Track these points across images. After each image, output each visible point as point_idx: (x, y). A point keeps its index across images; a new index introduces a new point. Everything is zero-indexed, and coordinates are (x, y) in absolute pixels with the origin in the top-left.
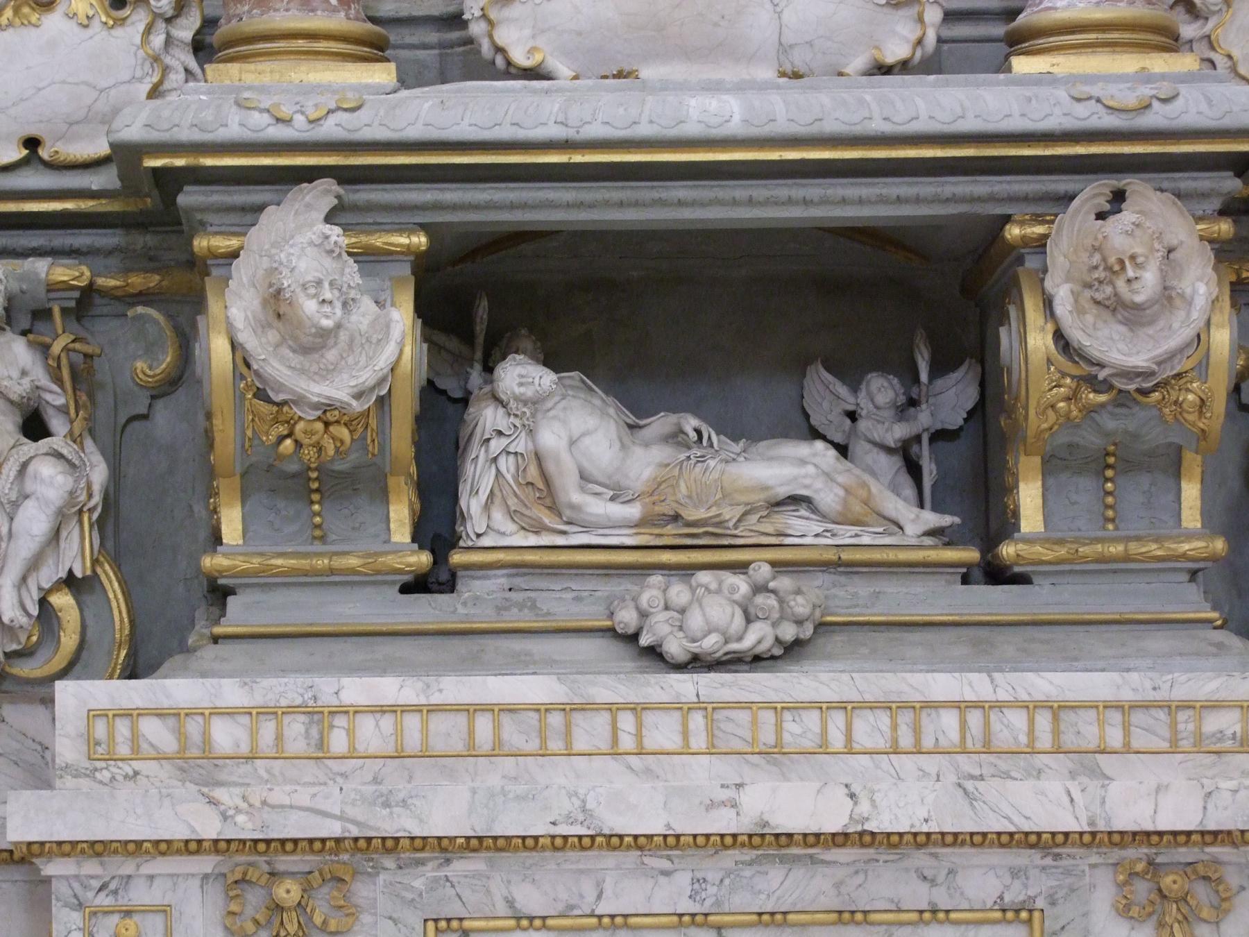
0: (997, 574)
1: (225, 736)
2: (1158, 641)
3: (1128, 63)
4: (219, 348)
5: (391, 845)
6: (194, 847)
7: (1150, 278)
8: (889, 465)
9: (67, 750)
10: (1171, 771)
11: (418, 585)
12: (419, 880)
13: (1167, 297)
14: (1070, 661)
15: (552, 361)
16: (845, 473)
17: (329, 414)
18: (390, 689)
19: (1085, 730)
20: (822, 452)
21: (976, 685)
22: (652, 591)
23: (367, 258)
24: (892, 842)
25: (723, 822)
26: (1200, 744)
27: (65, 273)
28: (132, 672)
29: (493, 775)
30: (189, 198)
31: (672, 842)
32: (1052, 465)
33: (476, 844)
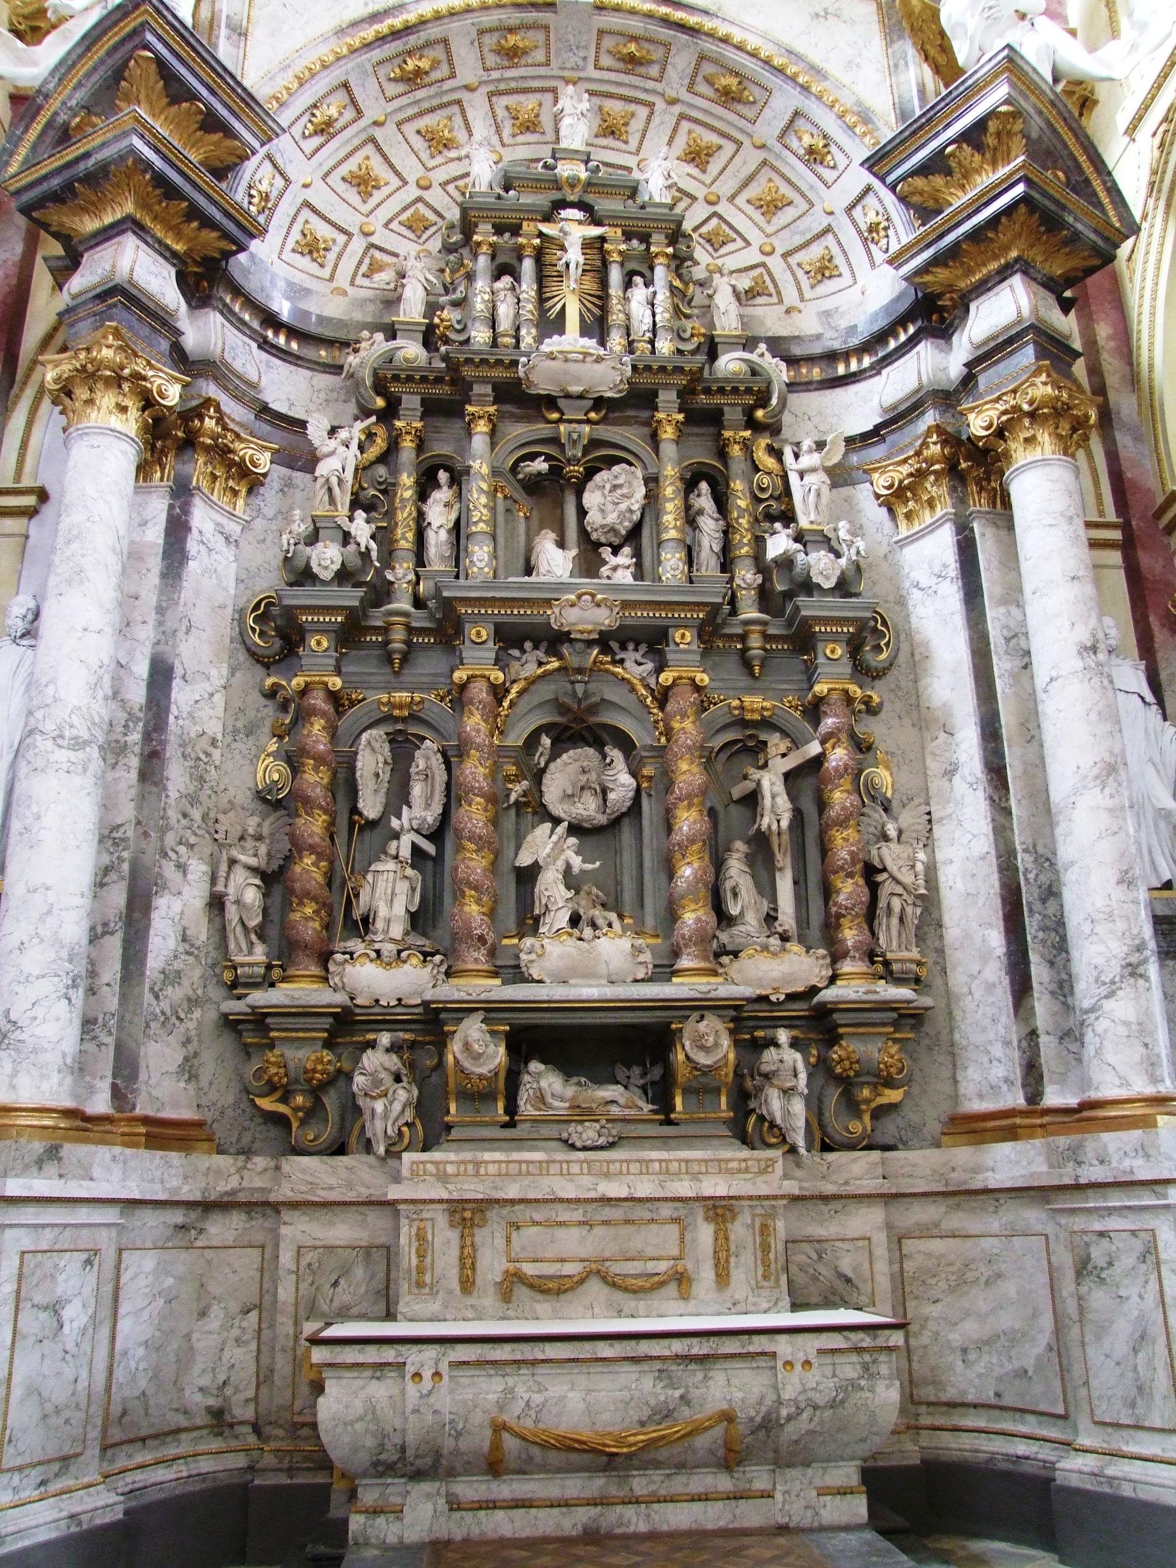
0: (669, 1122)
1: (450, 1169)
2: (715, 1142)
3: (705, 980)
4: (450, 1058)
5: (497, 1201)
6: (441, 1201)
7: (711, 1039)
8: (638, 1091)
9: (405, 1172)
10: (719, 1179)
11: (505, 1126)
12: (505, 1211)
13: (716, 1045)
14: (690, 1148)
15: (544, 1061)
16: (627, 1094)
17: (481, 1077)
18: (498, 1156)
19: (695, 1167)
20: (620, 1088)
21: (664, 1155)
22: (572, 1128)
23: (492, 1033)
24: (640, 1200)
25: (593, 1195)
27: (408, 1036)
28: (424, 1150)
29: (526, 1181)
30: (443, 1016)
31: (578, 1201)
32: (686, 1092)
33: (522, 1201)
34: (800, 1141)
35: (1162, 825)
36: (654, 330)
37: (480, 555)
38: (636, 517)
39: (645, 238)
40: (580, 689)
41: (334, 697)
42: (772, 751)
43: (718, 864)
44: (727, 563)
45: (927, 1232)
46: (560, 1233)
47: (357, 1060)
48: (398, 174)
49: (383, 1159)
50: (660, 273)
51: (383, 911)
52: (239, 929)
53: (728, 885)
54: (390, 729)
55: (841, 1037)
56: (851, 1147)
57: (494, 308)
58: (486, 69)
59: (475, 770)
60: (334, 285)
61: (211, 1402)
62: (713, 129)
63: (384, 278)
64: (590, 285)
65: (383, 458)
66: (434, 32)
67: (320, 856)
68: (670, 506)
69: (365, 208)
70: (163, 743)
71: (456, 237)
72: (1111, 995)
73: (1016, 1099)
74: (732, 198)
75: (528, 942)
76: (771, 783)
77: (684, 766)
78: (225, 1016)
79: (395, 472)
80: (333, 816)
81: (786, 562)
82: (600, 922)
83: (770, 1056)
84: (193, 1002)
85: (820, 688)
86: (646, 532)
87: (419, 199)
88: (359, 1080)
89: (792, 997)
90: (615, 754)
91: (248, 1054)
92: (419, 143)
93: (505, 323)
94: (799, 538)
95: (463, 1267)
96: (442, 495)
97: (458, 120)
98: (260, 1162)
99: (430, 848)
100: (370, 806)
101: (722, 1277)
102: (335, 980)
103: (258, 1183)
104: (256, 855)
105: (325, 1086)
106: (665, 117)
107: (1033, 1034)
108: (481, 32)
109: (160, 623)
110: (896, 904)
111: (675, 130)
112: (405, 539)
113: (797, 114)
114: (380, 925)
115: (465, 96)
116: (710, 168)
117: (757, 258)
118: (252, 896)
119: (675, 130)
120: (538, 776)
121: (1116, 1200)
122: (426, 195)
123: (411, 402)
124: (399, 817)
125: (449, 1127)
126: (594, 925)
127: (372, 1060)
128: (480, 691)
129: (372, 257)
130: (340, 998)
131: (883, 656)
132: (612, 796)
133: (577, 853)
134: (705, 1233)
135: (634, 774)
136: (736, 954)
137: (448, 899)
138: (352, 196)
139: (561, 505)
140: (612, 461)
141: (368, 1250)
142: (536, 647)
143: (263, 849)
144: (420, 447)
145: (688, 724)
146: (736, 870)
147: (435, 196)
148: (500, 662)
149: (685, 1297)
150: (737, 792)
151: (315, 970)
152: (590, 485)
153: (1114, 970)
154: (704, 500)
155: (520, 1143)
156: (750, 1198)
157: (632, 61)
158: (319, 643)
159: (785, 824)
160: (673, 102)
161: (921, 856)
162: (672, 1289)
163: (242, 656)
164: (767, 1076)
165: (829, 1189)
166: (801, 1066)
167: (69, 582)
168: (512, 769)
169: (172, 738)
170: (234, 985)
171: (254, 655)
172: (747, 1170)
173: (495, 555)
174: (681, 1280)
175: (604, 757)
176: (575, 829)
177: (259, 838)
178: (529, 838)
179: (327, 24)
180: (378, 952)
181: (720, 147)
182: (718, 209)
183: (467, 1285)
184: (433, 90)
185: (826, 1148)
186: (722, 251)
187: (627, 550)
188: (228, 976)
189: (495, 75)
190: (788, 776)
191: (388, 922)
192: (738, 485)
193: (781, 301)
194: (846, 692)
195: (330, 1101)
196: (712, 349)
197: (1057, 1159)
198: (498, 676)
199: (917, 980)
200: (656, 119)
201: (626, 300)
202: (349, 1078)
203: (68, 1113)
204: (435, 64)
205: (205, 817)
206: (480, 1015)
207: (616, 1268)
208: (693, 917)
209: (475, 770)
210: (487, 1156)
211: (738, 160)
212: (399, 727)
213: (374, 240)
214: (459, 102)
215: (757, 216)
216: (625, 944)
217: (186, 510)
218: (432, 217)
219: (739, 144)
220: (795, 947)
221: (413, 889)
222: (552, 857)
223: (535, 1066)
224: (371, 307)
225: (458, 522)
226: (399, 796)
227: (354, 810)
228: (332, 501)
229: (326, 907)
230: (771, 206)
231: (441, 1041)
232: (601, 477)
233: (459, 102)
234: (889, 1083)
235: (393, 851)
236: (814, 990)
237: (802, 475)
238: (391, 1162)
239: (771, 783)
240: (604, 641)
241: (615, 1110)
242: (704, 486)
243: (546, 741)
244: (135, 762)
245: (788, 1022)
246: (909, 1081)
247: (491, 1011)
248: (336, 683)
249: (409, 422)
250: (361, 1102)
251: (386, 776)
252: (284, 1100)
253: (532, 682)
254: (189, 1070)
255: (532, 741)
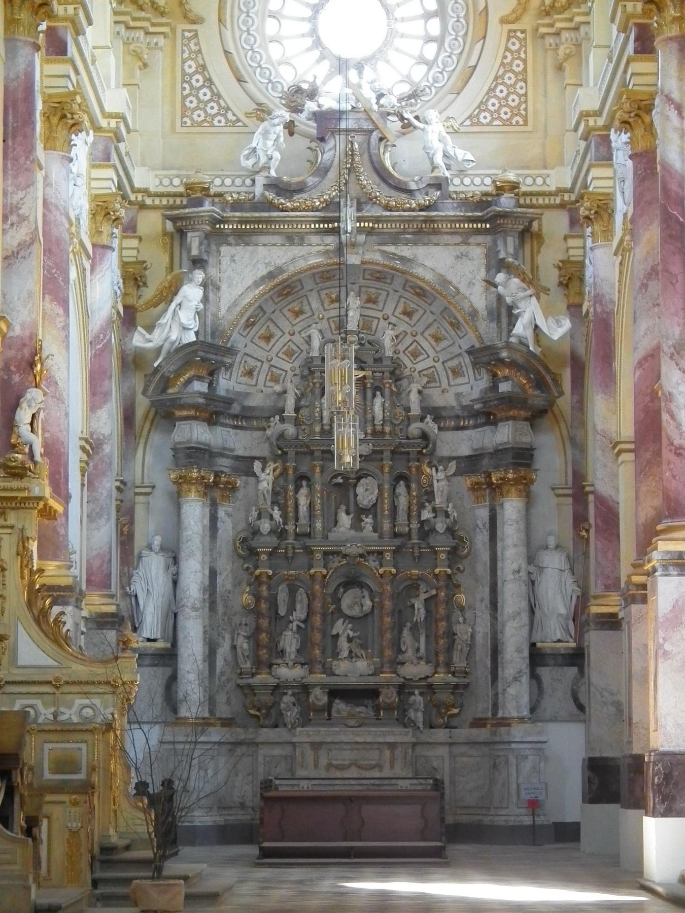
0: (380, 719)
1: (311, 733)
7: (390, 695)
8: (371, 708)
9: (297, 733)
11: (328, 720)
13: (392, 696)
14: (384, 727)
18: (325, 729)
20: (364, 708)
23: (323, 692)
26: (396, 735)
27: (297, 691)
31: (348, 743)
32: (385, 709)
34: (421, 726)
35: (560, 618)
36: (384, 420)
37: (318, 525)
38: (375, 502)
39: (383, 373)
40: (353, 571)
41: (270, 577)
42: (421, 591)
43: (400, 632)
44: (409, 517)
45: (463, 755)
46: (344, 752)
47: (281, 699)
48: (281, 330)
49: (290, 730)
50: (387, 391)
51: (288, 650)
52: (241, 656)
53: (402, 640)
54: (287, 583)
55: (435, 693)
56: (440, 727)
57: (322, 413)
58: (317, 284)
59: (317, 605)
60: (258, 387)
61: (241, 800)
62: (414, 303)
63: (278, 388)
64: (360, 400)
65: (281, 474)
66: (294, 279)
67: (267, 633)
68: (386, 501)
69: (268, 348)
70: (216, 598)
71: (306, 372)
72: (509, 686)
73: (490, 715)
74: (422, 334)
75: (335, 663)
76: (419, 604)
77: (387, 602)
78: (238, 685)
79: (286, 480)
80: (270, 618)
81: (428, 521)
82: (359, 654)
83: (413, 698)
84: (228, 680)
85: (437, 571)
86: (379, 505)
87: (290, 340)
88: (283, 705)
89: (421, 679)
90: (366, 593)
91: (246, 697)
92: (288, 314)
93: (325, 421)
94: (434, 510)
95: (315, 762)
96: (304, 491)
97: (305, 302)
98: (251, 730)
99: (303, 625)
100: (282, 611)
101: (392, 767)
102: (273, 673)
103: (251, 737)
104: (246, 632)
105: (271, 707)
106: (393, 297)
107: (497, 694)
108: (314, 275)
109: (211, 555)
110: (459, 647)
111: (398, 301)
112: (291, 509)
113: (445, 308)
114: (287, 654)
115: (308, 294)
116: (413, 318)
117: (433, 363)
118: (245, 646)
119: (398, 301)
120: (340, 600)
121: (502, 747)
122: (294, 338)
123: (291, 454)
124: (292, 616)
125: (310, 720)
126: (357, 656)
127: (288, 699)
128: (319, 576)
129: (272, 371)
130: (276, 681)
131: (466, 551)
132: (364, 608)
133: (351, 630)
134: (387, 753)
135: (372, 601)
136: (403, 664)
137: (309, 645)
138: (263, 344)
139: (348, 490)
140: (366, 476)
141: (286, 757)
142: (338, 556)
143: (248, 629)
144: (295, 469)
145: (388, 588)
146: (406, 633)
147: (296, 338)
148: (325, 567)
149: (381, 771)
150: (409, 604)
151: (267, 670)
152: (359, 484)
153: (511, 679)
154: (401, 489)
155: (332, 725)
156: (401, 743)
157: (378, 279)
158: (264, 557)
159: (422, 619)
160: (397, 291)
161: (470, 630)
162: (377, 769)
163: (236, 557)
164: (411, 705)
165: (431, 740)
166: (422, 701)
167: (189, 556)
168: (329, 600)
169: (218, 596)
170: (241, 674)
171: (239, 556)
172: (401, 734)
173: (323, 522)
174: (379, 766)
175: (363, 592)
176: (352, 619)
177: (246, 625)
178: (336, 624)
179: (250, 282)
180: (287, 664)
181: (417, 310)
182: (417, 338)
183: (316, 766)
184: (295, 295)
185: (431, 727)
186: (418, 360)
187: (371, 516)
188: (238, 671)
189: (321, 285)
190: (426, 600)
191: (290, 653)
192: (413, 486)
193: (440, 387)
194: (446, 571)
195: (273, 711)
196: (409, 420)
197: (494, 734)
198: (324, 572)
199: (466, 673)
200: (390, 297)
201: (373, 405)
202: (279, 704)
203: (204, 719)
204: (296, 286)
205: (229, 619)
206: (319, 687)
207: (360, 763)
208: (388, 653)
209: (317, 605)
210: (322, 729)
211: (425, 317)
212: (291, 582)
213: (272, 363)
214: (306, 296)
215: (433, 343)
216: (365, 663)
217: (216, 512)
218: (295, 348)
219: (425, 311)
220: (423, 663)
221: (297, 641)
222: (344, 632)
223: (337, 701)
224: (273, 397)
225: (310, 503)
226: (292, 608)
227: (277, 613)
228: (265, 499)
229: (270, 649)
230: (438, 339)
231: (308, 694)
232: (363, 481)
233: (306, 296)
234: (453, 706)
235: (290, 627)
236: (427, 677)
237: (438, 481)
238: (293, 730)
239: (419, 604)
240: (361, 556)
241: (362, 715)
242: (402, 483)
243: (342, 590)
244: (207, 605)
245: (417, 687)
246: (462, 706)
247: (323, 686)
248: (270, 572)
249: (291, 464)
250: (283, 712)
251: (287, 599)
252: (259, 710)
253: (336, 569)
254: (228, 702)
255: (337, 589)
